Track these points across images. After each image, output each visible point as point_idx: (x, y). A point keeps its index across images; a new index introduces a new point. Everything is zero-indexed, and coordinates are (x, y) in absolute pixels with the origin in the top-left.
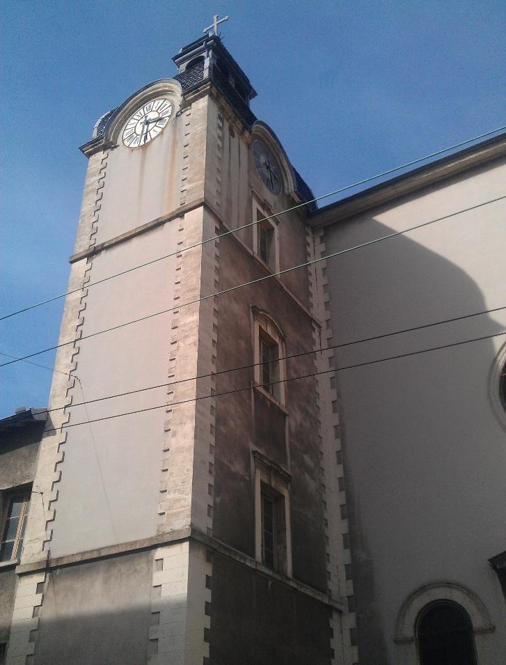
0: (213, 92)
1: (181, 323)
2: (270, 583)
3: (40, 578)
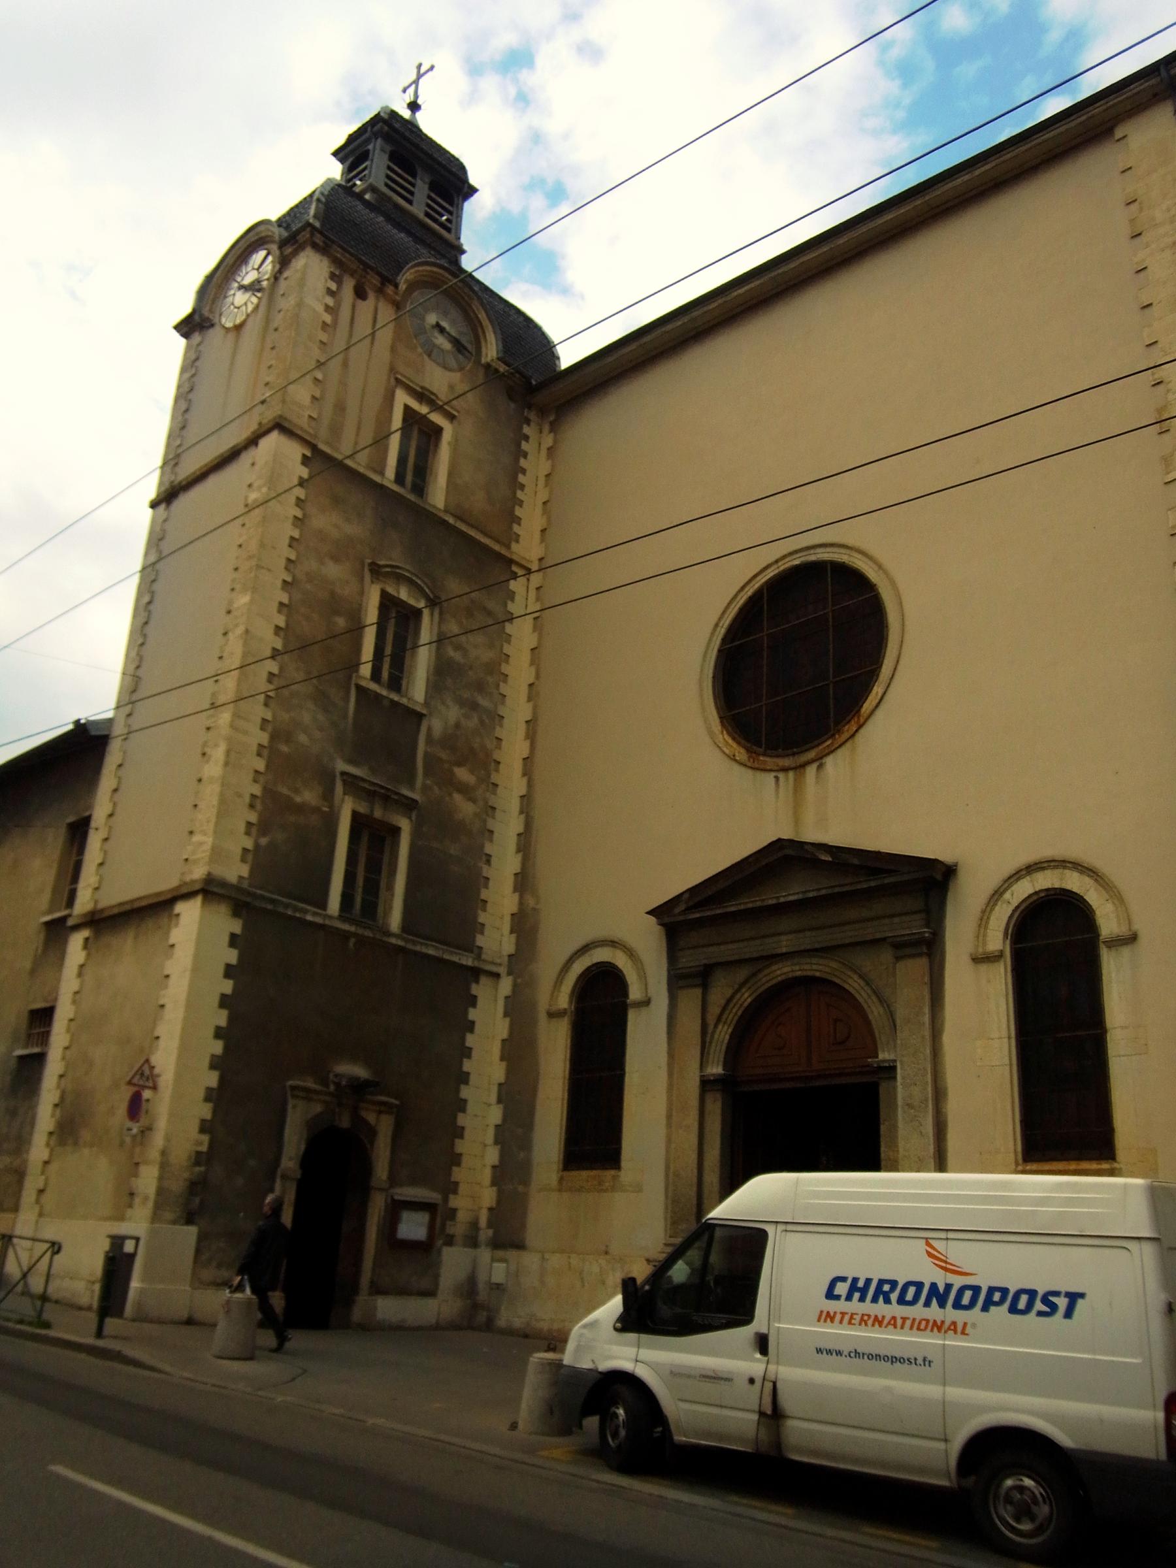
0: (318, 241)
1: (235, 606)
2: (352, 941)
3: (86, 933)
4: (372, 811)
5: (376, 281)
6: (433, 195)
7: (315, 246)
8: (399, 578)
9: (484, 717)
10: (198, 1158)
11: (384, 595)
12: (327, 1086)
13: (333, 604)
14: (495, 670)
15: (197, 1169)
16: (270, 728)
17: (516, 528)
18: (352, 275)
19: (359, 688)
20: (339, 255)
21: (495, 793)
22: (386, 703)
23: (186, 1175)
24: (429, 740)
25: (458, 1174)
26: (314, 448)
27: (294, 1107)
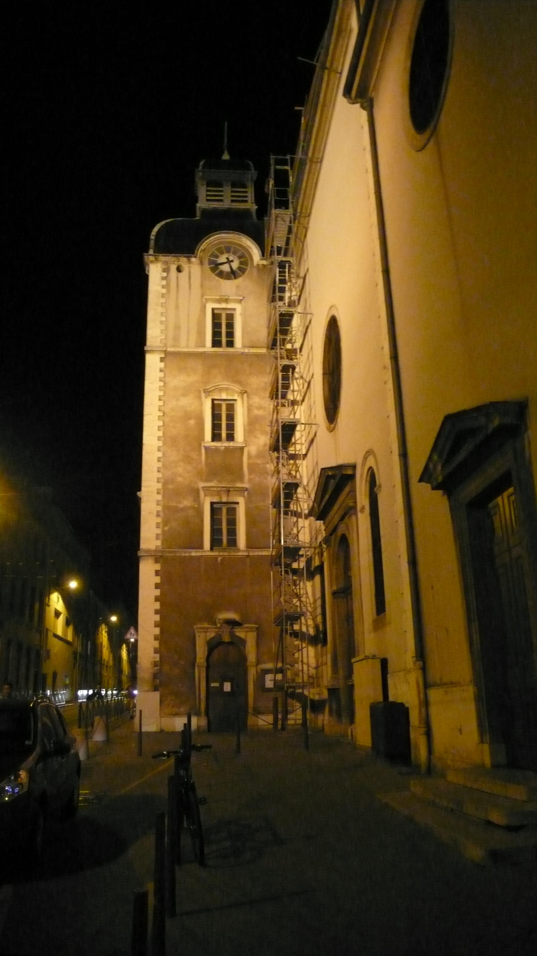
5: (185, 259)
6: (235, 189)
10: (155, 664)
12: (216, 625)
13: (187, 416)
15: (156, 668)
16: (162, 480)
18: (174, 264)
19: (206, 448)
23: (151, 671)
24: (249, 457)
26: (165, 352)
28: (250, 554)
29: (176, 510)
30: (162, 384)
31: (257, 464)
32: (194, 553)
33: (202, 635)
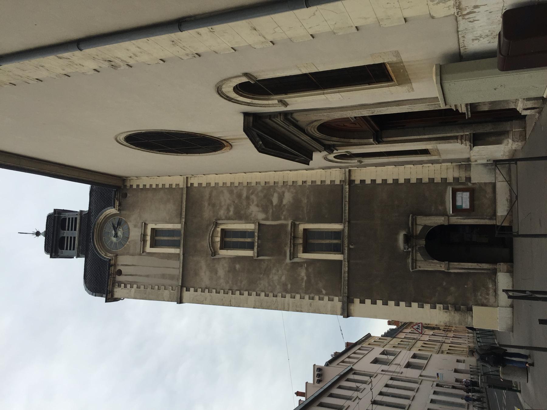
2: (351, 247)
4: (301, 244)
7: (112, 295)
8: (213, 243)
9: (251, 192)
10: (446, 308)
11: (221, 248)
13: (232, 270)
14: (231, 188)
15: (450, 308)
16: (284, 294)
17: (174, 186)
18: (115, 278)
20: (111, 286)
21: (278, 183)
22: (260, 242)
23: (453, 313)
24: (266, 219)
25: (438, 180)
26: (182, 287)
27: (420, 267)
28: (347, 220)
29: (308, 281)
30: (207, 290)
31: (273, 212)
32: (345, 269)
33: (419, 264)
